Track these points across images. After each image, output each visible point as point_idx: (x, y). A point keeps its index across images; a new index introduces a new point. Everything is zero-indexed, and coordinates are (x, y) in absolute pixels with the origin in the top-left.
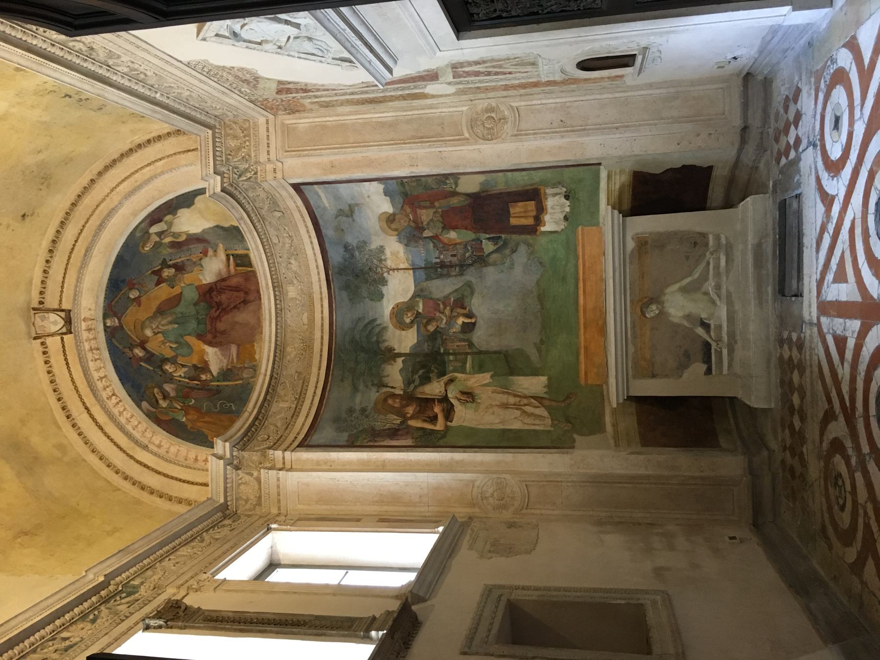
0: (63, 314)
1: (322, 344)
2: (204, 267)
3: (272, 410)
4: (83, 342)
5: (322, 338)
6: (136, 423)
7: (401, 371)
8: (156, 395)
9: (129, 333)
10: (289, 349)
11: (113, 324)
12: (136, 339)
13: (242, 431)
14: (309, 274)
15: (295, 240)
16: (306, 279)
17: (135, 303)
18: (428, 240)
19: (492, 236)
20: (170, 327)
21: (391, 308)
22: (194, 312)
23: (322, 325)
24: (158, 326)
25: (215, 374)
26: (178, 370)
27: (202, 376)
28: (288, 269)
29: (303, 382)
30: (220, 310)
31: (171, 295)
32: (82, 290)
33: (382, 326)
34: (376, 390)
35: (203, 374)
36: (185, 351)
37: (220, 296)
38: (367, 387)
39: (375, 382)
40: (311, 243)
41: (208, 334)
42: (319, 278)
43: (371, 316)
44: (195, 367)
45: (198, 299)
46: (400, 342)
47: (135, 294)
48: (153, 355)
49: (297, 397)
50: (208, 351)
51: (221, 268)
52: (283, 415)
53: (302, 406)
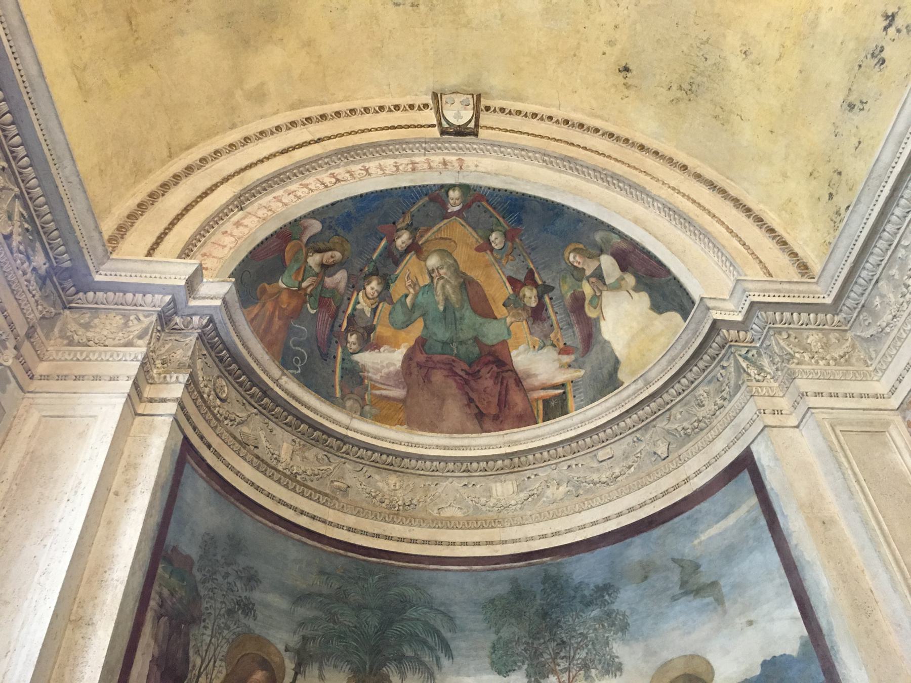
0: (472, 125)
1: (401, 540)
2: (540, 352)
3: (278, 429)
4: (425, 155)
5: (413, 541)
8: (330, 253)
9: (435, 229)
10: (393, 479)
11: (451, 202)
12: (424, 239)
13: (244, 352)
14: (541, 518)
15: (608, 488)
16: (529, 513)
17: (482, 242)
20: (440, 298)
22: (463, 336)
23: (440, 543)
24: (443, 278)
26: (368, 301)
27: (354, 336)
28: (546, 481)
29: (326, 495)
30: (465, 376)
31: (491, 302)
32: (508, 159)
33: (435, 668)
34: (292, 644)
35: (358, 339)
36: (400, 317)
37: (490, 378)
38: (302, 624)
39: (311, 645)
40: (607, 519)
41: (426, 355)
42: (532, 539)
43: (459, 644)
44: (371, 329)
45: (485, 345)
47: (497, 241)
48: (397, 263)
49: (299, 478)
51: (539, 378)
52: (264, 443)
53: (278, 481)
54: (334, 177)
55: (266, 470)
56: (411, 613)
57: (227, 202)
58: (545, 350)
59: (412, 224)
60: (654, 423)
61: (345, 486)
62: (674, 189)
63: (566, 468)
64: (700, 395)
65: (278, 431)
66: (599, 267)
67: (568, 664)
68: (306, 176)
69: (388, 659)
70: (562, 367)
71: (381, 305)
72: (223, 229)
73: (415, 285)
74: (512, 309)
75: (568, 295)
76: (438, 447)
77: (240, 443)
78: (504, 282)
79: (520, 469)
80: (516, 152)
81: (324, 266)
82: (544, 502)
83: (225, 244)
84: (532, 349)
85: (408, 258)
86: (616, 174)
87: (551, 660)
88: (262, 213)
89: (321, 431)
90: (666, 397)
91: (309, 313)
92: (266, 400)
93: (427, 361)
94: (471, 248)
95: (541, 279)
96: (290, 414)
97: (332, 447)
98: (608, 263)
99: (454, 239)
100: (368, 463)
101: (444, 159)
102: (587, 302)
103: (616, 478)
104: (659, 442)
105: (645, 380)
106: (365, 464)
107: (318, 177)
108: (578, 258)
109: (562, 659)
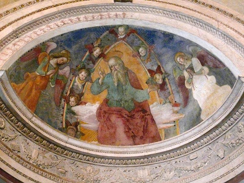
2: (163, 105)
4: (107, 11)
6: (38, 33)
8: (61, 58)
9: (112, 46)
13: (12, 105)
15: (194, 174)
20: (115, 80)
22: (127, 99)
25: (76, 109)
29: (54, 175)
32: (147, 13)
35: (75, 99)
36: (96, 89)
44: (82, 95)
47: (142, 52)
48: (94, 63)
49: (41, 167)
50: (94, 106)
52: (23, 149)
53: (30, 169)
54: (63, 22)
55: (23, 163)
57: (9, 34)
58: (166, 105)
59: (101, 44)
60: (218, 140)
61: (65, 171)
62: (226, 25)
63: (174, 163)
64: (240, 126)
65: (31, 143)
66: (192, 64)
68: (50, 22)
70: (173, 113)
71: (87, 83)
72: (7, 47)
73: (103, 74)
74: (150, 85)
75: (177, 79)
76: (112, 152)
77: (10, 149)
78: (146, 72)
79: (152, 163)
80: (151, 9)
81: (58, 65)
82: (163, 180)
83: (7, 53)
84: (159, 105)
85: (99, 60)
86: (198, 19)
88: (26, 39)
89: (53, 144)
90: (223, 127)
91: (51, 87)
92: (25, 129)
93: (109, 110)
94: (130, 56)
95: (164, 70)
96: (37, 135)
97: (59, 152)
98: (195, 62)
99: (121, 51)
100: (77, 160)
101: (116, 14)
102: (186, 81)
103: (199, 168)
104: (220, 150)
105: (213, 119)
106: (76, 160)
107: (55, 23)
108: (181, 60)
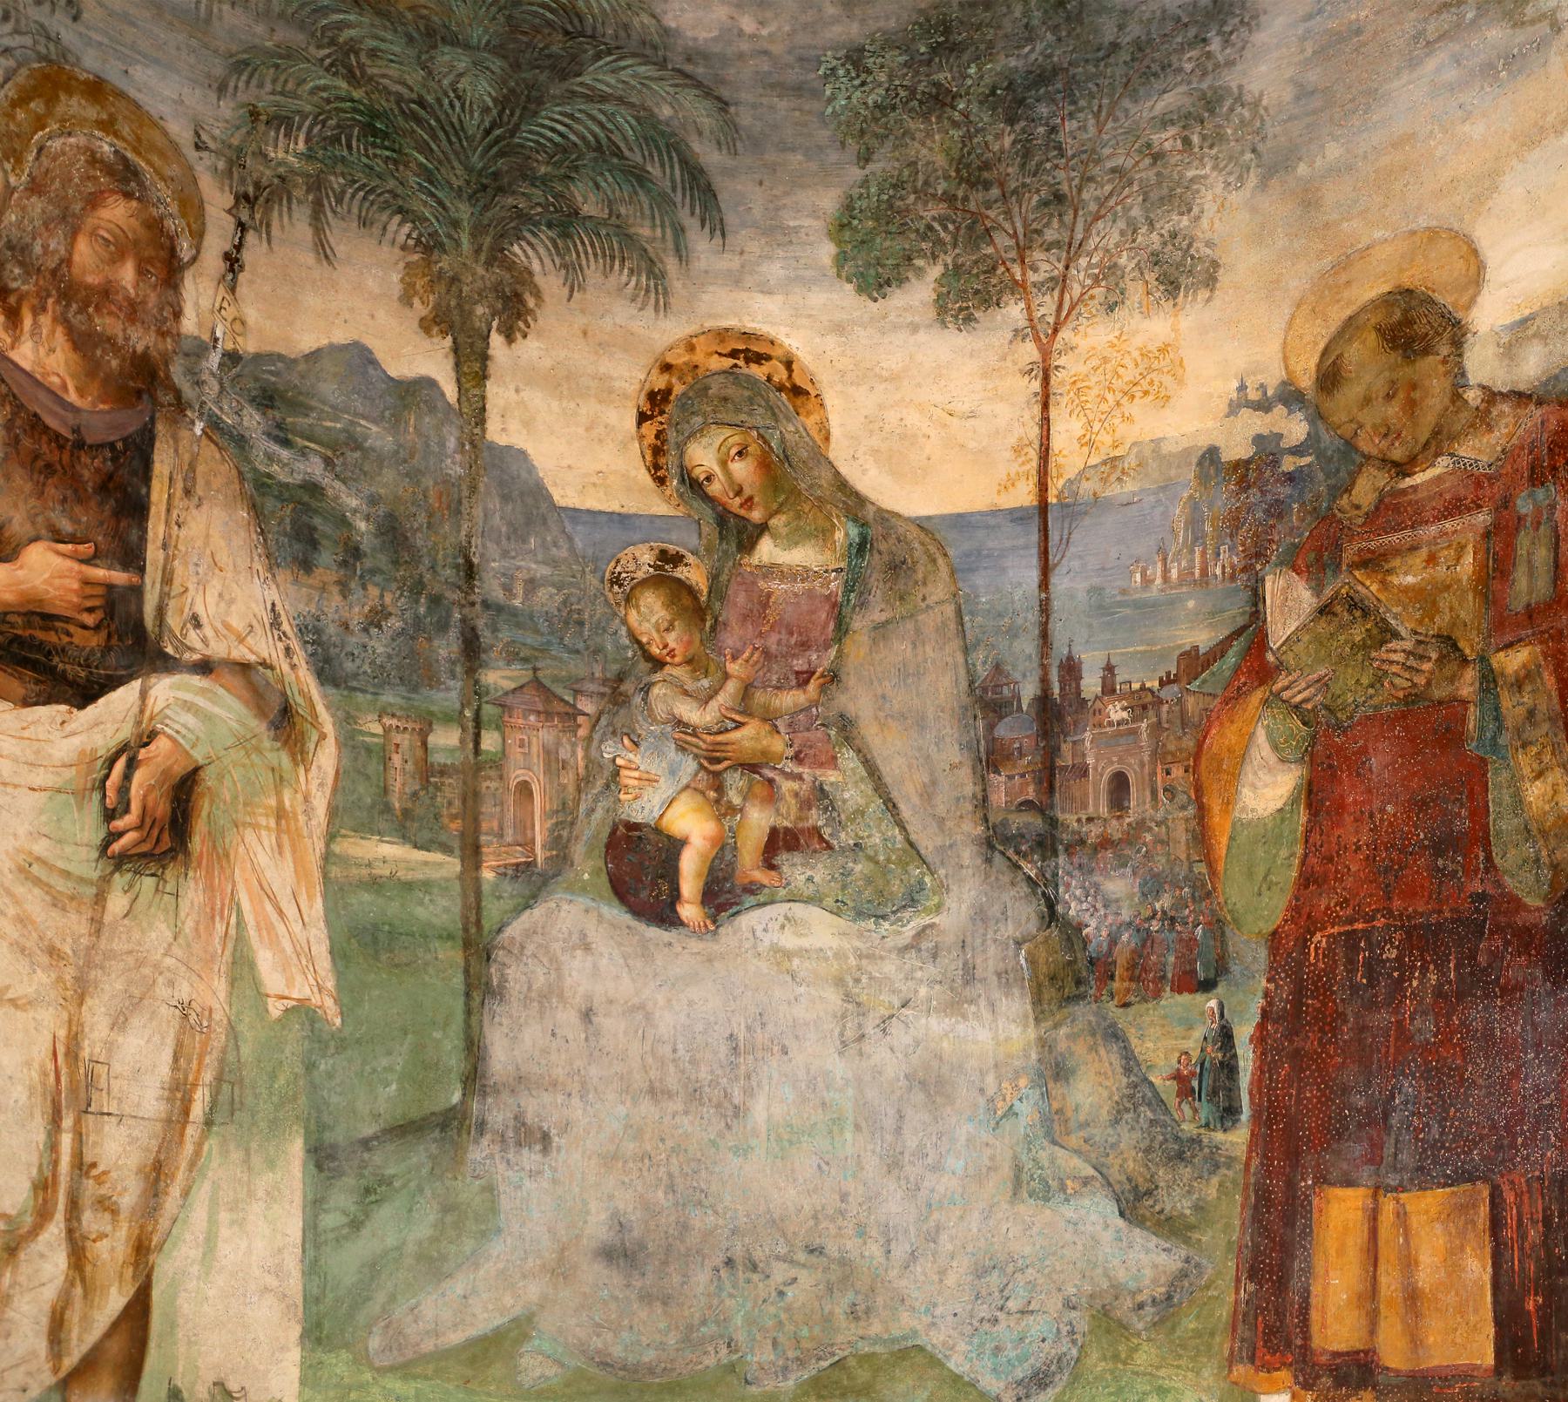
7: (359, 358)
18: (1236, 612)
19: (1246, 1058)
21: (795, 341)
46: (561, 382)
56: (599, 76)
67: (1061, 266)
69: (522, 217)
87: (1013, 254)
109: (1047, 250)
